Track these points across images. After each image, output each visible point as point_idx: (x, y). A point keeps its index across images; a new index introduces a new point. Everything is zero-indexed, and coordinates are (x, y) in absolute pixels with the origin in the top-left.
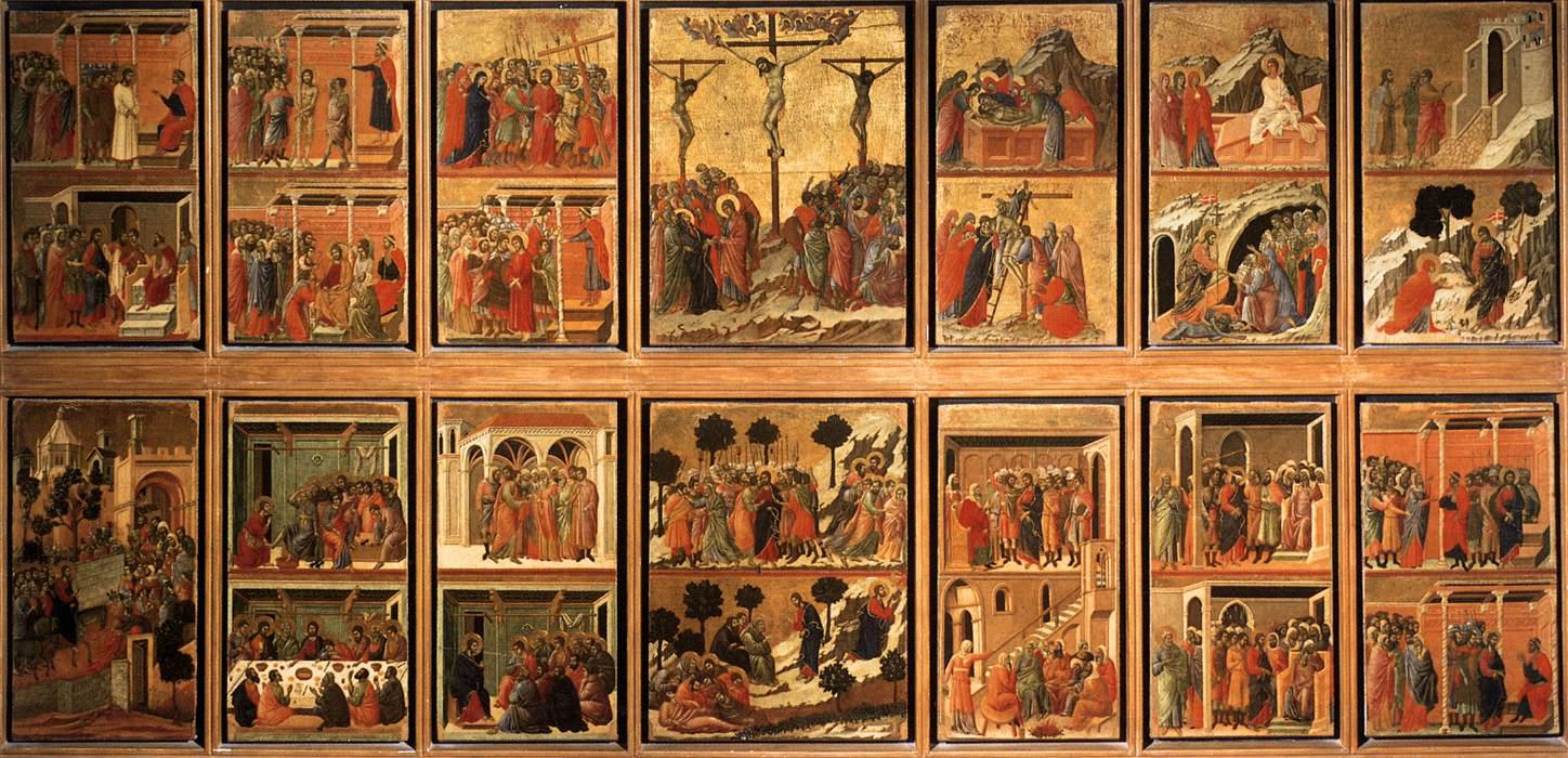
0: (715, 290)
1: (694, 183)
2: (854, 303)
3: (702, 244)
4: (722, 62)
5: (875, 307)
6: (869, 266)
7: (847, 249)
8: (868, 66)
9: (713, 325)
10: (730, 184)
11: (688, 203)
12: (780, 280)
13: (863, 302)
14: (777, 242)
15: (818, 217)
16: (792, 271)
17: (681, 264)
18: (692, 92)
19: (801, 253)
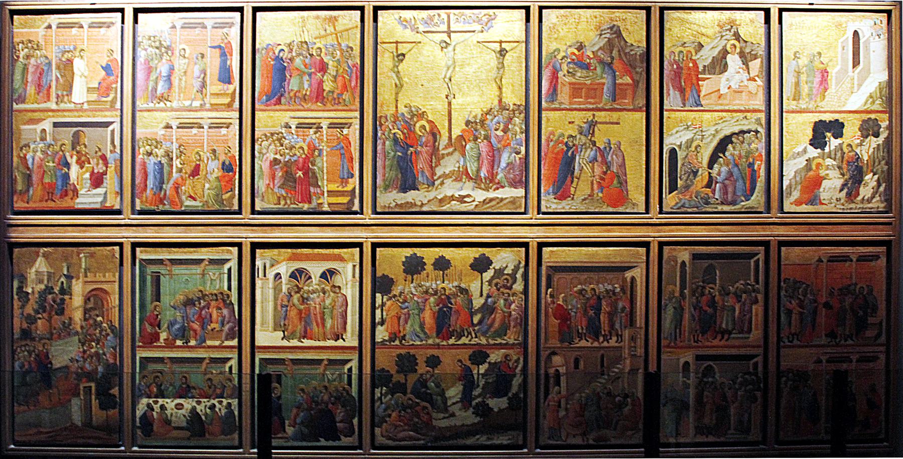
0: (415, 178)
2: (495, 186)
3: (408, 150)
4: (420, 42)
5: (507, 189)
6: (503, 164)
7: (491, 154)
8: (504, 45)
10: (422, 115)
12: (453, 172)
13: (500, 186)
14: (451, 150)
16: (459, 167)
19: (464, 155)
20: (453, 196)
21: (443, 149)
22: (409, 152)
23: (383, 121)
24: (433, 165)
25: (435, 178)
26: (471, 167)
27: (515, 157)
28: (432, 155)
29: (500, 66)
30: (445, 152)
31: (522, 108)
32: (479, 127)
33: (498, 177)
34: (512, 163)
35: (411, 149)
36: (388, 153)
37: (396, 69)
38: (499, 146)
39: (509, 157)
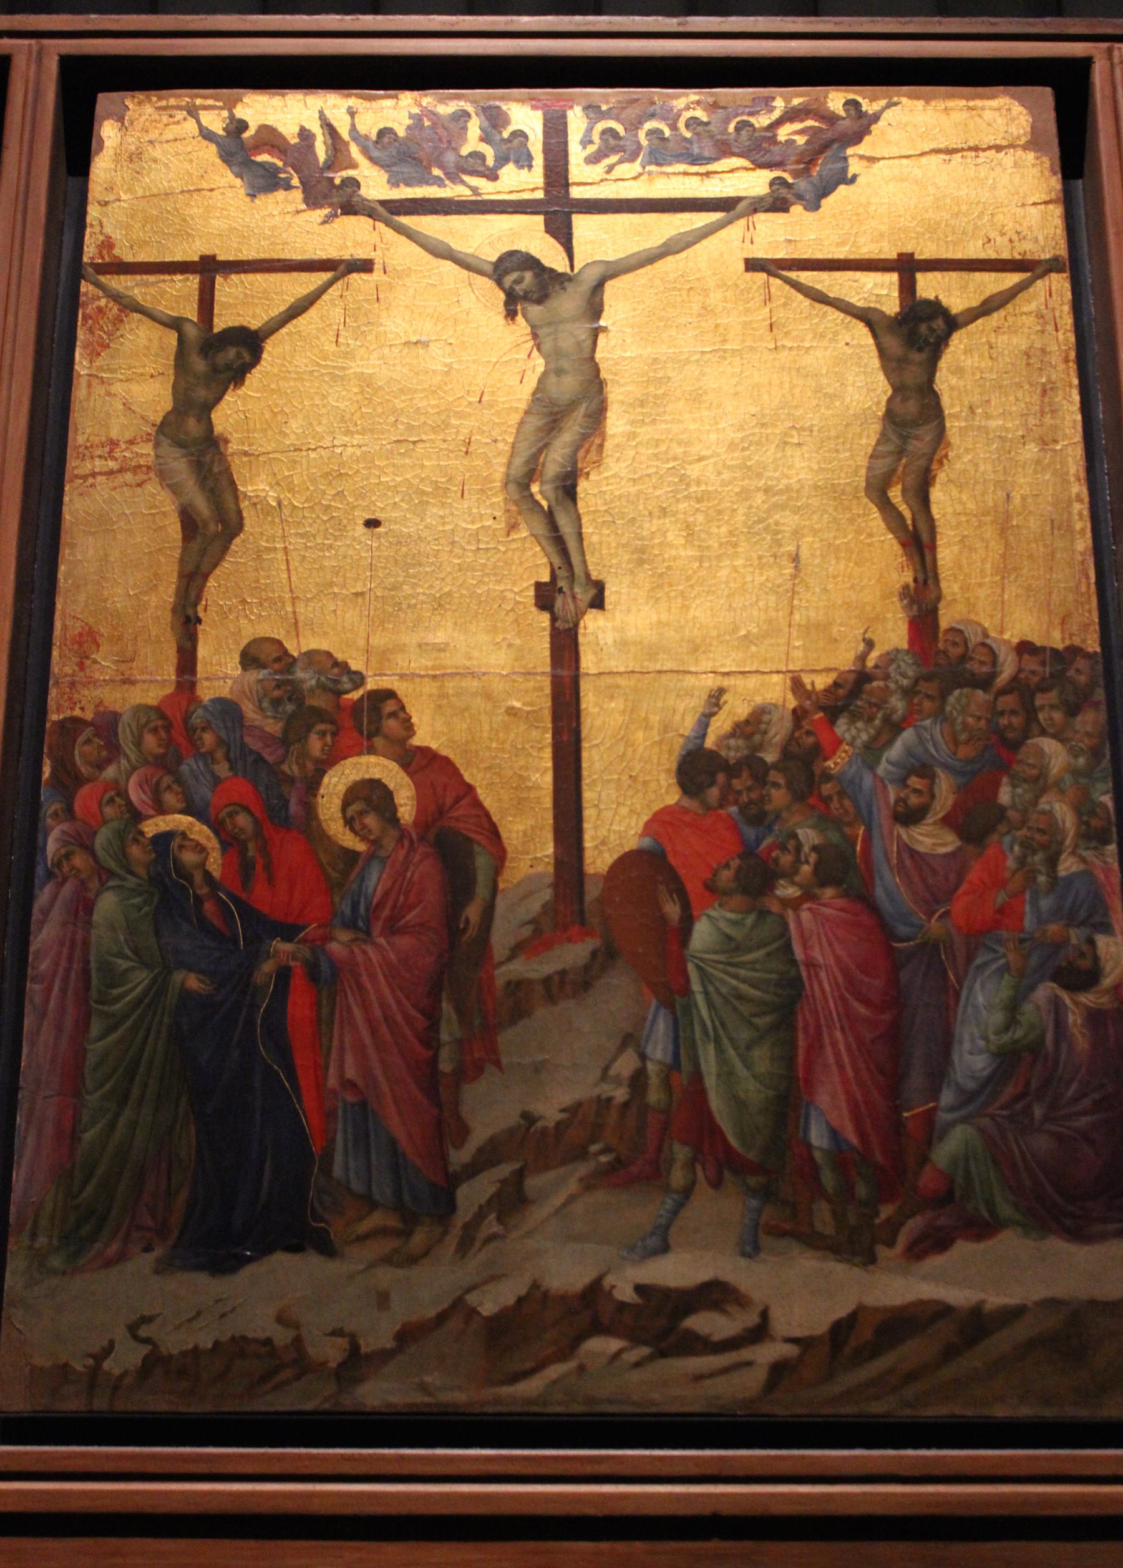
1: (228, 710)
2: (914, 1225)
4: (366, 266)
5: (1009, 1242)
8: (928, 286)
9: (282, 1319)
11: (204, 792)
15: (748, 852)
16: (638, 1080)
18: (238, 375)
20: (594, 1291)
21: (517, 950)
22: (268, 967)
23: (82, 754)
24: (446, 1066)
25: (459, 1157)
26: (727, 1075)
27: (1057, 1008)
28: (435, 993)
29: (911, 407)
30: (518, 968)
31: (1080, 673)
32: (779, 797)
33: (944, 1153)
34: (1035, 1048)
35: (281, 947)
36: (113, 978)
37: (193, 426)
38: (934, 927)
39: (1013, 1008)
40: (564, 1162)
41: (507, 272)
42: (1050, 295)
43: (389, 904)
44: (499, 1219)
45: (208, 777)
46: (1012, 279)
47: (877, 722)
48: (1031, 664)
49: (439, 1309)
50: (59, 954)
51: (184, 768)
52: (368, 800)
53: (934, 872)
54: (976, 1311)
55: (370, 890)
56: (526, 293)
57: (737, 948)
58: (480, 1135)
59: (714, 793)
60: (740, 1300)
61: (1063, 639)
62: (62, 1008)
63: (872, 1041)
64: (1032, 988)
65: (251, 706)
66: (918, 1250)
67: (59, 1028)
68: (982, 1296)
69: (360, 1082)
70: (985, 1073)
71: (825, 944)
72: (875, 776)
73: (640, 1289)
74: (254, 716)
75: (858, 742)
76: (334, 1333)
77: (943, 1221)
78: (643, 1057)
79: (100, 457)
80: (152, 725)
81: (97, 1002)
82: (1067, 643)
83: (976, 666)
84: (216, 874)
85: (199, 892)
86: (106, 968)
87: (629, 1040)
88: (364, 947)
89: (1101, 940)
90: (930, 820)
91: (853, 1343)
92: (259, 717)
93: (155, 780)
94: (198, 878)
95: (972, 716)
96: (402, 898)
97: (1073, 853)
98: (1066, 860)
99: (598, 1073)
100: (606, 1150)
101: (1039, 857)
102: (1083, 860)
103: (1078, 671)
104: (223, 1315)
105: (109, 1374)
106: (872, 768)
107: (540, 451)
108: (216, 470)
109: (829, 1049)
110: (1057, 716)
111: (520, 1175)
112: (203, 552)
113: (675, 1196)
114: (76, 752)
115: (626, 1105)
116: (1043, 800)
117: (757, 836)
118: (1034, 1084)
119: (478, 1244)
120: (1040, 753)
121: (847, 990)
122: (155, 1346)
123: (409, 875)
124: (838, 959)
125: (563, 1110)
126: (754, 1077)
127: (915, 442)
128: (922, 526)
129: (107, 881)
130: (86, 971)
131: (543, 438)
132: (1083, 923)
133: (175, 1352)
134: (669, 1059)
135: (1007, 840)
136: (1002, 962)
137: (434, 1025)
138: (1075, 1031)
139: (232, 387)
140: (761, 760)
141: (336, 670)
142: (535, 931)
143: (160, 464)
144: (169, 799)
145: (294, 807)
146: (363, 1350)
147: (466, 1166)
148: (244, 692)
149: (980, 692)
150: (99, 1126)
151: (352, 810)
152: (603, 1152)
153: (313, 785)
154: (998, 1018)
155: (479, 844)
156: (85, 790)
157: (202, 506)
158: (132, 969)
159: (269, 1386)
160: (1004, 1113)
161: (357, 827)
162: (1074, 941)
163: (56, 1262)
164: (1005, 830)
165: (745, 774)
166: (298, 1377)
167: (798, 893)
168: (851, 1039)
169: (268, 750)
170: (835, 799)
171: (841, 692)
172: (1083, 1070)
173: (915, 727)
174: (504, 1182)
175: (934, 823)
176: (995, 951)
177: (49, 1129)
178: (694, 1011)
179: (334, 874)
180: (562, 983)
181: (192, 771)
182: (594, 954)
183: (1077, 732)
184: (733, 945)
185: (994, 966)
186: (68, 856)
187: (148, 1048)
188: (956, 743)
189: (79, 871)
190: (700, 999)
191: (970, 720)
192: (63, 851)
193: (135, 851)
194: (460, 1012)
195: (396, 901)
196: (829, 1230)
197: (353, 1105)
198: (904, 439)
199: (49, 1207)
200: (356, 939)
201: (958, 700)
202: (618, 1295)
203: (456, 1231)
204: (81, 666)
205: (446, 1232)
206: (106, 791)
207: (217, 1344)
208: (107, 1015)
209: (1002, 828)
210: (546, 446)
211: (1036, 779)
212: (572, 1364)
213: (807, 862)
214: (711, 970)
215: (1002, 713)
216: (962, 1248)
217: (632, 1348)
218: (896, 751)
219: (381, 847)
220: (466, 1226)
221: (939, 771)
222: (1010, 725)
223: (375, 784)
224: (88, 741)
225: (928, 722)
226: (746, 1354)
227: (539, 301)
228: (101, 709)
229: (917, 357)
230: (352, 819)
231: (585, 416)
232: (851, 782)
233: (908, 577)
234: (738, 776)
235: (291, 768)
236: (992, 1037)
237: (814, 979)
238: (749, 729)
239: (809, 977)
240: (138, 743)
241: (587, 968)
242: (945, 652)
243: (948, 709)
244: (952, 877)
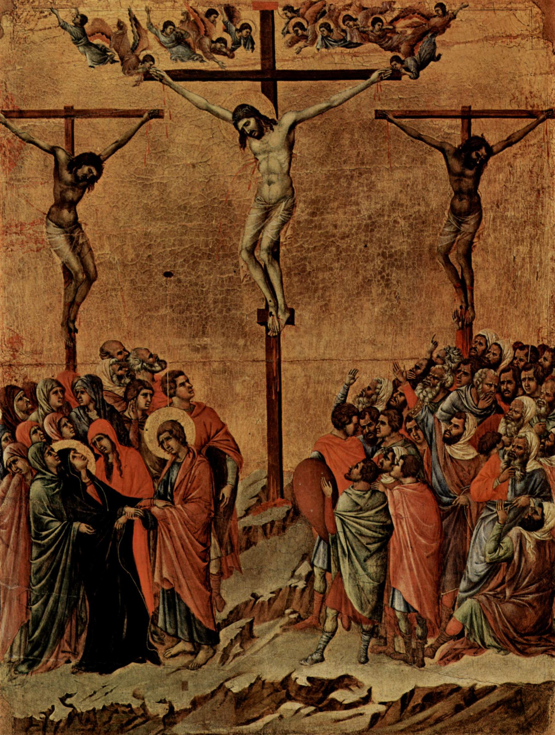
5: (490, 654)
16: (310, 577)
17: (66, 560)
22: (122, 520)
24: (213, 570)
29: (465, 204)
30: (250, 521)
32: (384, 429)
35: (129, 510)
37: (66, 214)
39: (499, 540)
40: (272, 618)
41: (240, 119)
42: (546, 133)
43: (183, 488)
44: (241, 646)
45: (86, 419)
46: (526, 122)
47: (437, 388)
48: (520, 354)
49: (213, 689)
50: (14, 514)
51: (73, 414)
52: (171, 432)
53: (463, 469)
54: (472, 689)
55: (173, 481)
56: (252, 131)
57: (361, 510)
58: (230, 606)
59: (350, 427)
60: (359, 685)
61: (538, 341)
62: (17, 544)
63: (428, 557)
64: (509, 529)
65: (107, 380)
66: (446, 659)
67: (16, 552)
68: (475, 682)
69: (171, 580)
70: (483, 573)
71: (405, 507)
72: (435, 418)
73: (309, 679)
74: (109, 385)
75: (427, 400)
76: (160, 702)
77: (458, 646)
78: (312, 565)
79: (16, 233)
80: (54, 390)
81: (34, 539)
82: (541, 343)
83: (491, 355)
84: (93, 471)
85: (84, 481)
86: (38, 520)
87: (304, 557)
88: (171, 509)
89: (546, 505)
90: (462, 441)
91: (412, 704)
92: (112, 386)
93: (57, 421)
94: (83, 473)
95: (487, 384)
96: (189, 484)
97: (535, 459)
98: (530, 464)
99: (290, 574)
100: (294, 612)
101: (517, 461)
102: (541, 463)
103: (545, 359)
104: (107, 693)
105: (52, 721)
106: (433, 412)
107: (259, 232)
108: (81, 241)
109: (405, 561)
110: (532, 384)
111: (251, 624)
112: (76, 291)
113: (327, 634)
114: (15, 405)
115: (303, 590)
116: (521, 431)
117: (372, 450)
118: (507, 578)
119: (231, 658)
120: (522, 405)
121: (416, 531)
122: (74, 708)
123: (193, 472)
124: (412, 515)
125: (272, 593)
126: (368, 575)
127: (466, 226)
128: (467, 276)
129: (36, 475)
130: (28, 523)
131: (260, 224)
132: (538, 496)
133: (84, 711)
134: (325, 567)
135: (502, 452)
136: (495, 516)
137: (207, 551)
138: (530, 552)
139: (87, 190)
140: (376, 409)
141: (151, 359)
142: (258, 501)
143: (49, 238)
144: (66, 430)
145: (131, 436)
146: (176, 709)
147: (224, 620)
148: (103, 372)
149: (492, 371)
150: (40, 602)
151: (162, 437)
152: (292, 613)
153: (141, 424)
154: (491, 545)
155: (229, 456)
156: (20, 427)
157: (75, 264)
158: (52, 521)
159: (130, 727)
160: (491, 593)
161: (166, 447)
162: (532, 505)
163: (23, 668)
164: (501, 447)
165: (367, 417)
166: (144, 723)
167: (393, 481)
168: (416, 556)
169: (117, 404)
170: (413, 430)
171: (419, 371)
172: (532, 572)
173: (457, 390)
174: (243, 628)
175: (464, 444)
176: (492, 511)
177: (15, 603)
178: (338, 542)
179: (154, 472)
180: (272, 527)
181: (77, 415)
182: (288, 512)
183: (541, 393)
184: (359, 508)
185: (491, 518)
186: (14, 462)
187: (63, 562)
188: (478, 399)
189: (21, 470)
190: (341, 535)
191: (486, 387)
192: (12, 459)
193: (49, 459)
194: (221, 544)
195: (187, 485)
196: (403, 651)
197: (167, 591)
198: (459, 223)
199: (17, 642)
200: (166, 506)
201: (480, 376)
202: (299, 682)
203: (220, 652)
204: (14, 356)
205: (215, 653)
206: (32, 427)
207: (104, 707)
208: (39, 545)
209: (499, 446)
210: (263, 228)
211: (518, 420)
212: (276, 715)
213: (398, 464)
214: (347, 520)
215: (503, 383)
216: (467, 658)
217: (305, 707)
218: (445, 405)
219: (178, 457)
220: (225, 650)
221: (468, 415)
222: (507, 389)
223: (174, 423)
224: (21, 399)
225: (463, 388)
226: (360, 709)
227: (259, 137)
228: (27, 381)
229: (469, 172)
230: (163, 442)
231: (284, 210)
232: (423, 420)
233: (457, 305)
234: (363, 418)
235: (129, 414)
236: (488, 555)
237: (399, 525)
238: (370, 392)
239: (397, 525)
240: (48, 400)
241: (285, 520)
242: (475, 349)
243: (475, 380)
244: (472, 472)
